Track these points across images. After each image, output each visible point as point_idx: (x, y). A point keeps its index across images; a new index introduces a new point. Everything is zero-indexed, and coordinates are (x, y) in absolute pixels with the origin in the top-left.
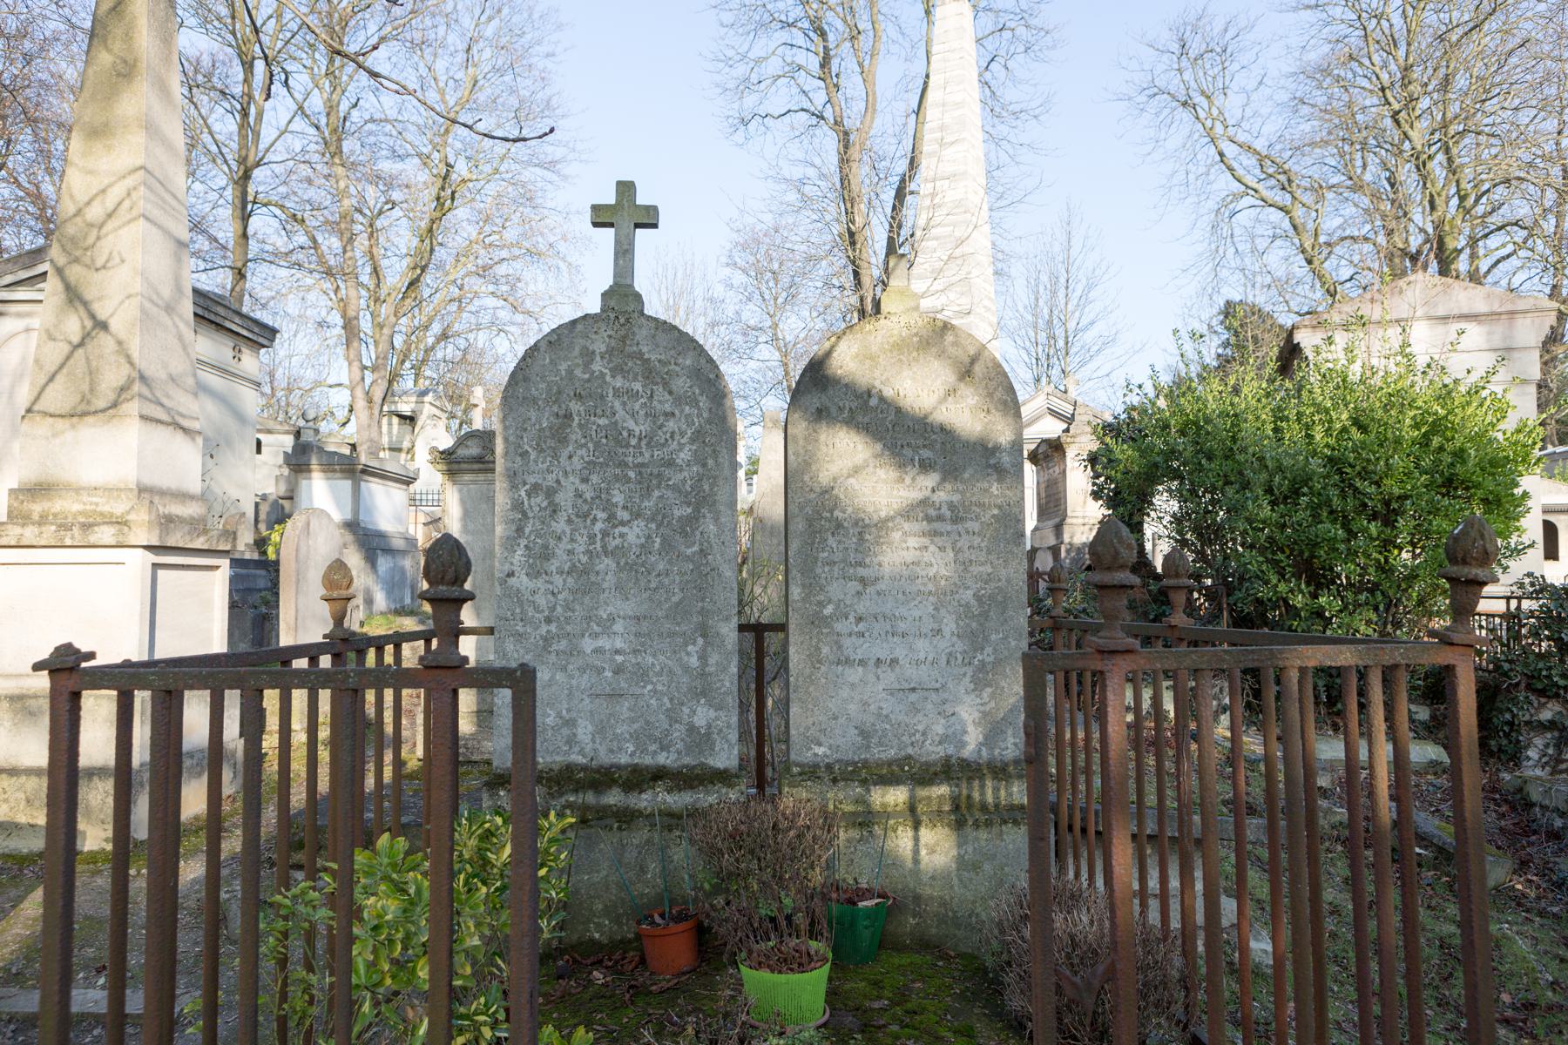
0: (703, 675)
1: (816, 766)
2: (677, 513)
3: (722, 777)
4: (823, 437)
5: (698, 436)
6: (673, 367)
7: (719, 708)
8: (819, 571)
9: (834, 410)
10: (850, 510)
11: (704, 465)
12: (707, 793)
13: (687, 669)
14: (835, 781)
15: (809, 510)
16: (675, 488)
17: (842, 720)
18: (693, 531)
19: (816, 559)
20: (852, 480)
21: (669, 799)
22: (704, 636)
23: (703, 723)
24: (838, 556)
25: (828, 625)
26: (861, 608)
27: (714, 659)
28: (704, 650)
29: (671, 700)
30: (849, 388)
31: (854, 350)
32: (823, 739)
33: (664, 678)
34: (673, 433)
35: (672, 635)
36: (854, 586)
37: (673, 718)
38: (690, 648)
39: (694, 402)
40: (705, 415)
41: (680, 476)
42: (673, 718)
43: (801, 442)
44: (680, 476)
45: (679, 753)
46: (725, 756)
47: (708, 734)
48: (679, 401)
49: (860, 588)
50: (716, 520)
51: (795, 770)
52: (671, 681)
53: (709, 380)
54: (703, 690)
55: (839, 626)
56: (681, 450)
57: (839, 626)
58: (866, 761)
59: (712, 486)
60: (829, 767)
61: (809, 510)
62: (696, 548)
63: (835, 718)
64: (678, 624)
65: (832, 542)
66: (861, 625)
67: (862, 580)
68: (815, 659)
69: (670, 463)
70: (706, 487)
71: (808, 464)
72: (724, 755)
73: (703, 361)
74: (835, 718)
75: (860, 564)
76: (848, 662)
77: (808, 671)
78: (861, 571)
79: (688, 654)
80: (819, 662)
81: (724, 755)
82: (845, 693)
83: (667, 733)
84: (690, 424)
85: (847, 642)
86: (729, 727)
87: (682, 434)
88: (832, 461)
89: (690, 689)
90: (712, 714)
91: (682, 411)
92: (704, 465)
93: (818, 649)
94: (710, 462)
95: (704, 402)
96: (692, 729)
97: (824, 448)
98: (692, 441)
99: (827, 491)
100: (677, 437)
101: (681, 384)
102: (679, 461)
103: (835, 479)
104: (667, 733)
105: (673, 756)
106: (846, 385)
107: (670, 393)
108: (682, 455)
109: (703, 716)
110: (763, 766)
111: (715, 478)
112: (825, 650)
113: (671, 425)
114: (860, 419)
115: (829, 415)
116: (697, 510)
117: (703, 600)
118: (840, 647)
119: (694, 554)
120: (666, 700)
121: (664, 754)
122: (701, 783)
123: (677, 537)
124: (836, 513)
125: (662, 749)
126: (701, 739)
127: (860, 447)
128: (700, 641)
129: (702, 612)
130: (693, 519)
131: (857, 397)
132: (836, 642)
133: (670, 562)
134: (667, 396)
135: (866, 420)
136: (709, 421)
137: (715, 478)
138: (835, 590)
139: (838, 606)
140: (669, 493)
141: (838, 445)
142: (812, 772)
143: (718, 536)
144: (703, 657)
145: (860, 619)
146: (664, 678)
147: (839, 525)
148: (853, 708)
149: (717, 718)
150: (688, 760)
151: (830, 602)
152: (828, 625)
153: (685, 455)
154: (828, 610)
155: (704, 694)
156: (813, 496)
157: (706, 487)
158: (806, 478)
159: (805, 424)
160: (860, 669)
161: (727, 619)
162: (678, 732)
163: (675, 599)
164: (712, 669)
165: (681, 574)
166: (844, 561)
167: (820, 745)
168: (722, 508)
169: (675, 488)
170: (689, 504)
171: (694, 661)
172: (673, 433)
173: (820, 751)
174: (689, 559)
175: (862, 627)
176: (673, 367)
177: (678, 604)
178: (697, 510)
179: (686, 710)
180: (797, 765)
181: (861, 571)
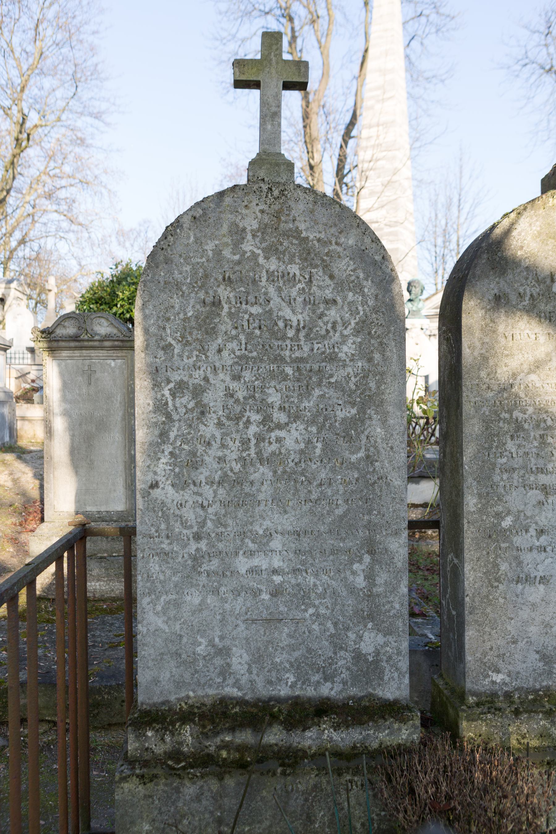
0: (370, 596)
1: (494, 695)
2: (341, 415)
3: (391, 710)
4: (501, 328)
5: (363, 327)
6: (333, 247)
7: (388, 633)
8: (497, 478)
9: (513, 297)
10: (531, 410)
11: (370, 360)
12: (378, 729)
13: (352, 590)
14: (517, 713)
15: (486, 410)
16: (337, 386)
17: (521, 644)
18: (358, 435)
19: (494, 465)
20: (533, 377)
21: (336, 736)
22: (371, 552)
23: (371, 649)
24: (518, 462)
25: (507, 539)
26: (543, 520)
27: (382, 578)
28: (371, 568)
29: (335, 624)
30: (531, 271)
31: (536, 228)
32: (501, 665)
33: (328, 601)
34: (334, 324)
35: (334, 551)
36: (535, 495)
37: (338, 644)
38: (356, 566)
39: (358, 288)
40: (371, 303)
41: (343, 373)
42: (338, 644)
43: (478, 334)
44: (343, 373)
45: (345, 683)
46: (395, 686)
47: (377, 662)
48: (341, 286)
49: (542, 497)
50: (384, 422)
51: (471, 700)
52: (335, 604)
53: (375, 263)
54: (371, 613)
55: (518, 540)
56: (344, 342)
57: (518, 540)
58: (548, 688)
59: (378, 384)
60: (508, 696)
61: (486, 410)
62: (361, 454)
63: (515, 642)
64: (343, 540)
65: (511, 445)
66: (543, 538)
67: (545, 489)
68: (493, 577)
69: (332, 358)
70: (373, 385)
71: (485, 359)
72: (394, 685)
73: (368, 240)
74: (515, 642)
75: (541, 470)
76: (528, 580)
77: (484, 591)
78: (543, 479)
79: (354, 573)
80: (498, 580)
81: (394, 685)
82: (525, 614)
83: (331, 661)
84: (354, 312)
85: (528, 558)
86: (399, 653)
87: (345, 324)
88: (511, 355)
89: (356, 612)
90: (380, 639)
91: (345, 298)
92: (370, 360)
93: (496, 566)
94: (377, 356)
95: (369, 288)
96: (358, 656)
97: (502, 340)
98: (357, 332)
99: (506, 388)
100: (339, 328)
101: (344, 267)
102: (342, 355)
103: (514, 375)
104: (331, 661)
105: (338, 687)
106: (527, 268)
107: (332, 277)
108: (345, 348)
109: (370, 641)
110: (440, 700)
111: (382, 374)
112: (504, 567)
113: (333, 314)
114: (542, 307)
115: (508, 302)
116: (362, 410)
117: (370, 513)
118: (520, 563)
119: (360, 460)
120: (329, 625)
121: (329, 684)
122: (371, 718)
123: (341, 442)
124: (516, 414)
125: (326, 680)
126: (369, 667)
127: (542, 339)
128: (367, 558)
129: (369, 526)
130: (358, 422)
131: (538, 281)
132: (516, 558)
133: (333, 470)
134: (328, 281)
135: (549, 308)
136: (375, 310)
137: (382, 374)
138: (515, 499)
139: (517, 519)
140: (331, 392)
141: (517, 337)
142: (490, 703)
143: (386, 440)
144: (370, 577)
145: (541, 532)
146: (328, 601)
147: (519, 427)
148: (534, 630)
149: (386, 644)
150: (354, 691)
151: (509, 513)
152: (507, 539)
153: (348, 349)
154: (507, 522)
155: (371, 617)
156: (490, 394)
157: (373, 385)
158: (483, 374)
159: (481, 313)
160: (542, 587)
161: (396, 533)
162: (344, 660)
163: (339, 512)
164: (381, 590)
165: (345, 483)
166: (524, 467)
167: (498, 671)
168: (390, 409)
169: (337, 386)
170: (353, 404)
171: (360, 581)
172: (334, 324)
173: (498, 678)
174: (353, 466)
175: (543, 540)
176: (333, 247)
177: (342, 518)
178: (362, 410)
179: (352, 635)
180: (474, 694)
181: (543, 479)
